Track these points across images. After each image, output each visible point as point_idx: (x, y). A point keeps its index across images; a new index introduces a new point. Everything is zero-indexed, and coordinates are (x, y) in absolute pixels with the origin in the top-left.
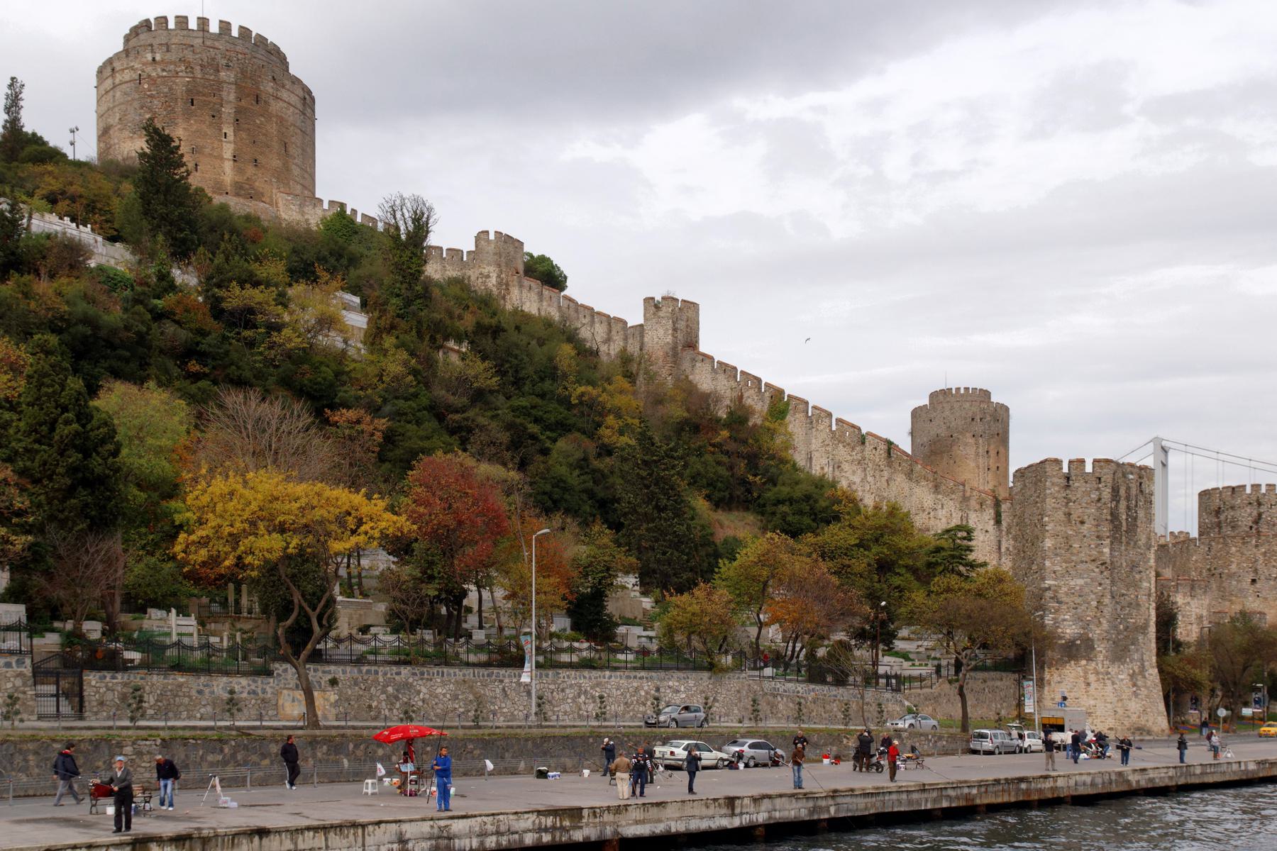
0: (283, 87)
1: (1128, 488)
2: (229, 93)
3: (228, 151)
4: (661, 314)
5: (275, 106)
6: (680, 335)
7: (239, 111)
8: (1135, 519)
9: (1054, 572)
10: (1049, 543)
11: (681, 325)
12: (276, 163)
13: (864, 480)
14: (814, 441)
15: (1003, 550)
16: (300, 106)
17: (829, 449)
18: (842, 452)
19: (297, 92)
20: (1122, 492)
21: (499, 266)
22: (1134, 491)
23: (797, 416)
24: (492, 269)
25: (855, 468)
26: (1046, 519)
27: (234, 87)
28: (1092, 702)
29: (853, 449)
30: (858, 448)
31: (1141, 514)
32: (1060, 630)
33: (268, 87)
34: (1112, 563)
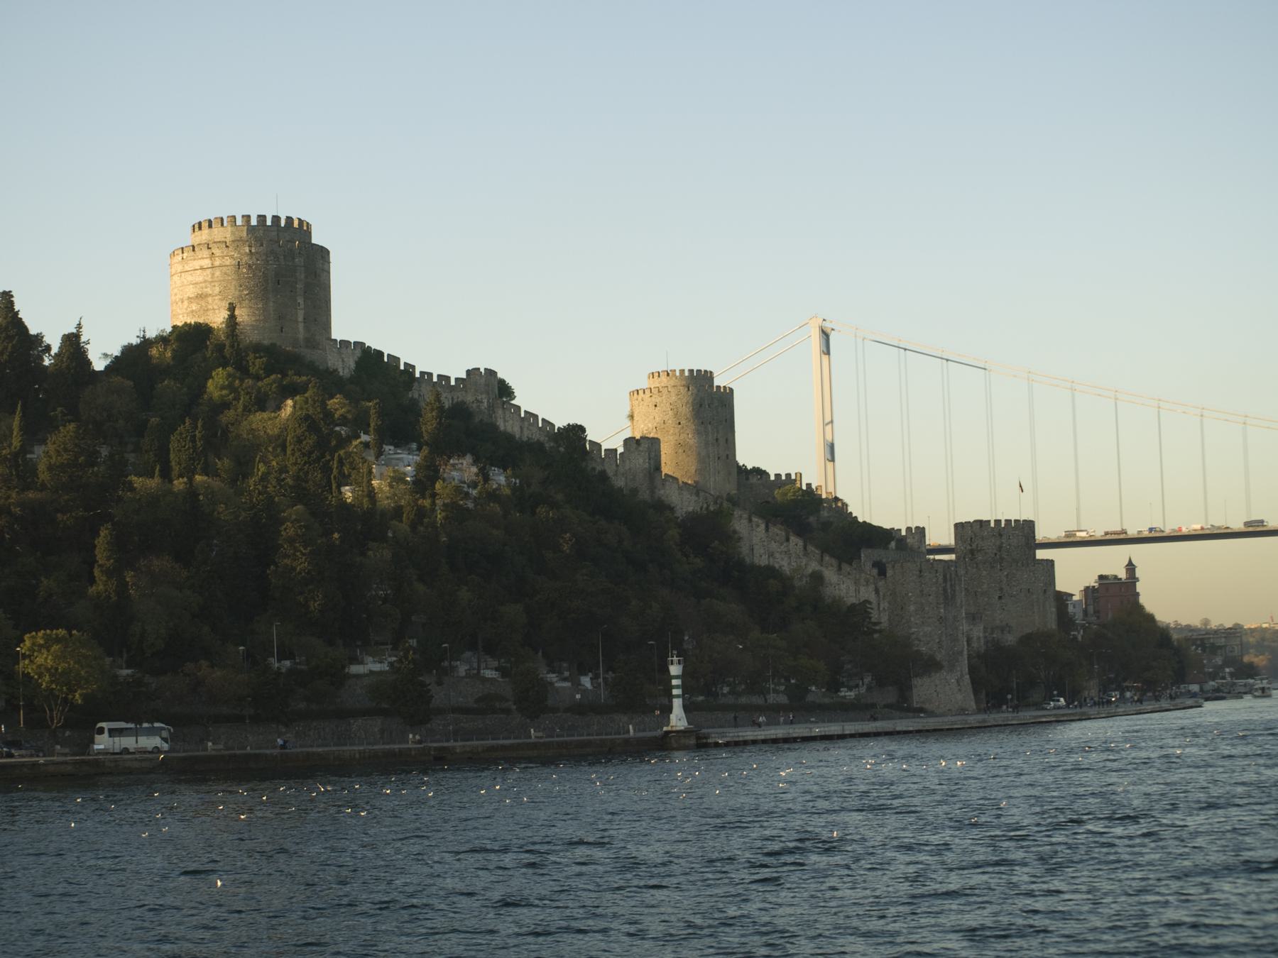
1: (951, 574)
3: (301, 319)
4: (641, 449)
6: (652, 462)
8: (954, 591)
9: (916, 624)
10: (912, 608)
11: (653, 454)
13: (789, 564)
14: (754, 538)
15: (881, 609)
17: (765, 544)
18: (774, 545)
20: (948, 576)
21: (488, 394)
22: (953, 576)
23: (742, 521)
24: (484, 396)
25: (783, 556)
26: (910, 594)
27: (303, 269)
29: (782, 544)
30: (785, 544)
31: (957, 588)
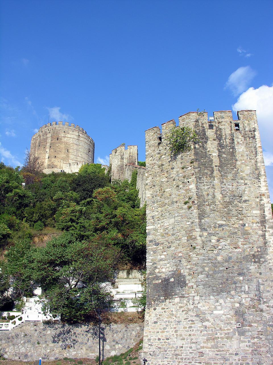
2: (49, 140)
3: (47, 156)
4: (117, 154)
7: (51, 144)
8: (233, 154)
12: (63, 155)
16: (76, 138)
19: (75, 134)
28: (180, 343)
31: (240, 149)
32: (157, 271)
33: (62, 135)
34: (199, 196)
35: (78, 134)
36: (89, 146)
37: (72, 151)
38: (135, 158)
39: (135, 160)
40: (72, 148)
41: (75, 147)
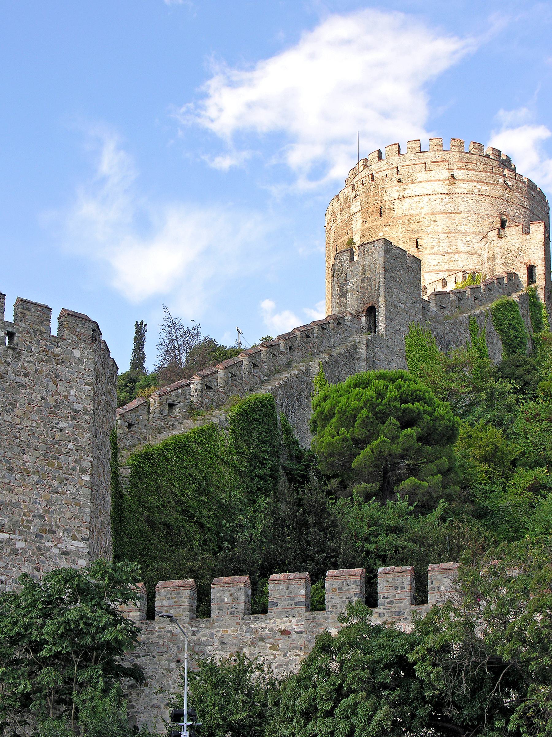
0: (413, 182)
5: (401, 209)
6: (351, 300)
16: (442, 188)
19: (437, 177)
33: (394, 192)
35: (446, 174)
36: (499, 202)
37: (432, 240)
38: (377, 284)
39: (378, 289)
40: (429, 230)
41: (443, 222)
